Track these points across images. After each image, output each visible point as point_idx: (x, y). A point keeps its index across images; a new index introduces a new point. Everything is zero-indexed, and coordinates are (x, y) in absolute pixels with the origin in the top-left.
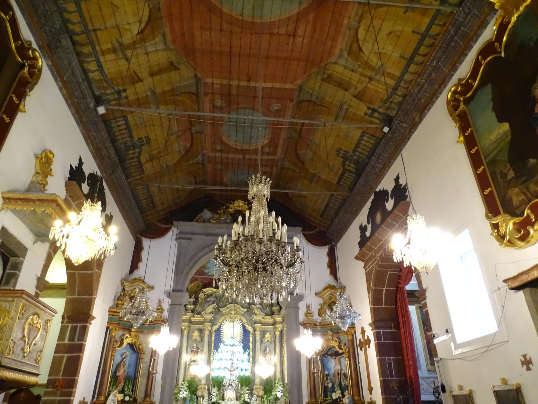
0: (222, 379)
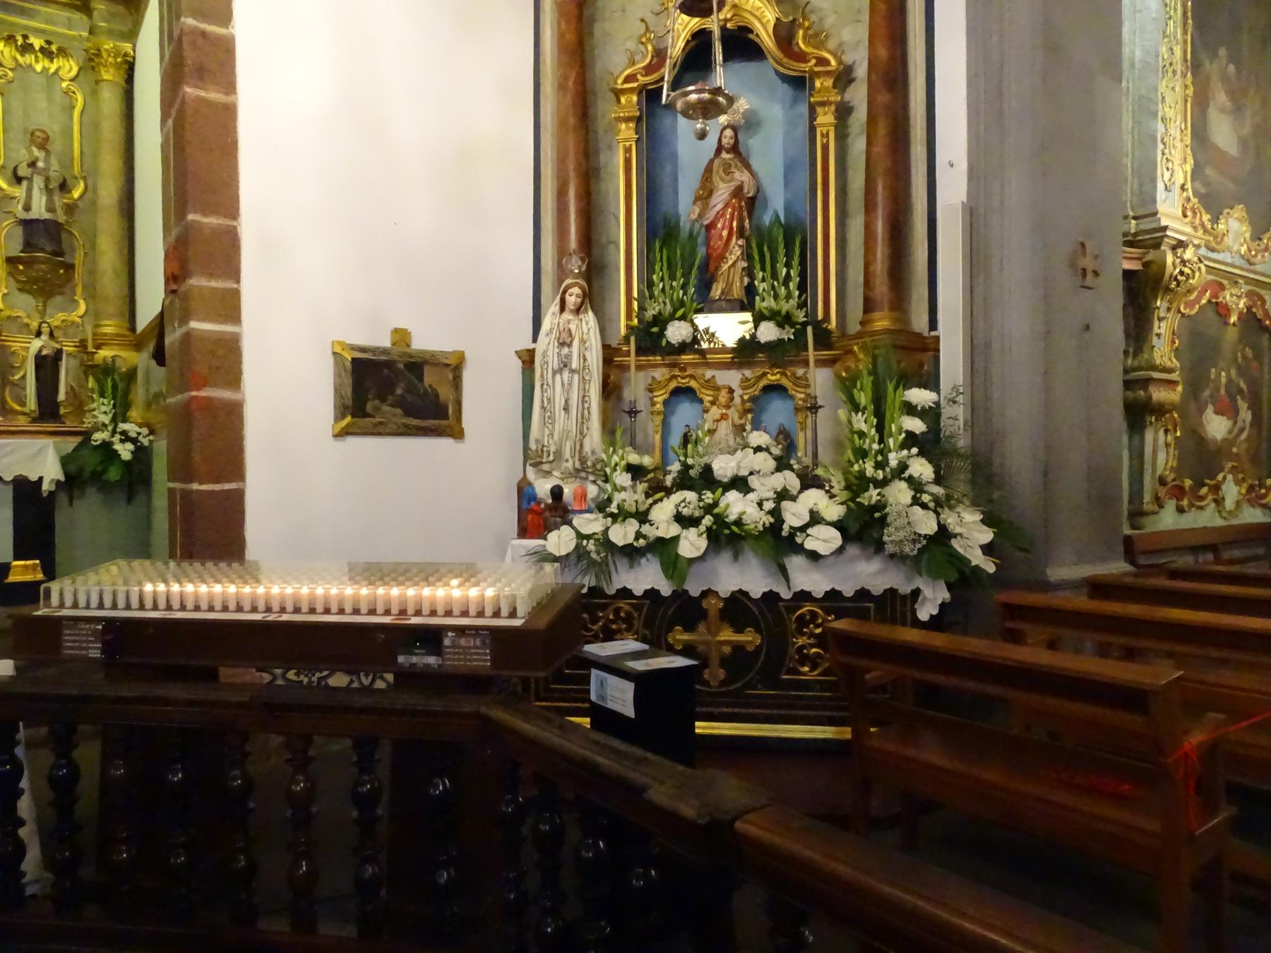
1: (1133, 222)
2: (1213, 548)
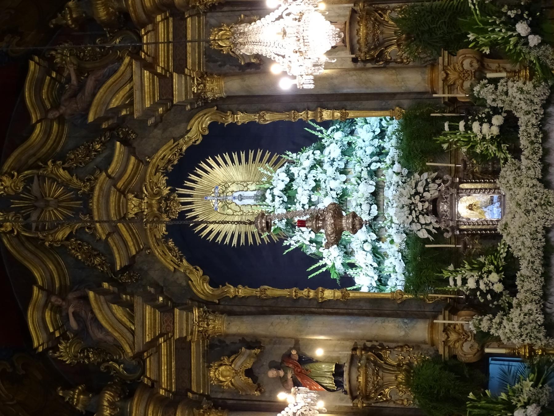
0: (412, 240)
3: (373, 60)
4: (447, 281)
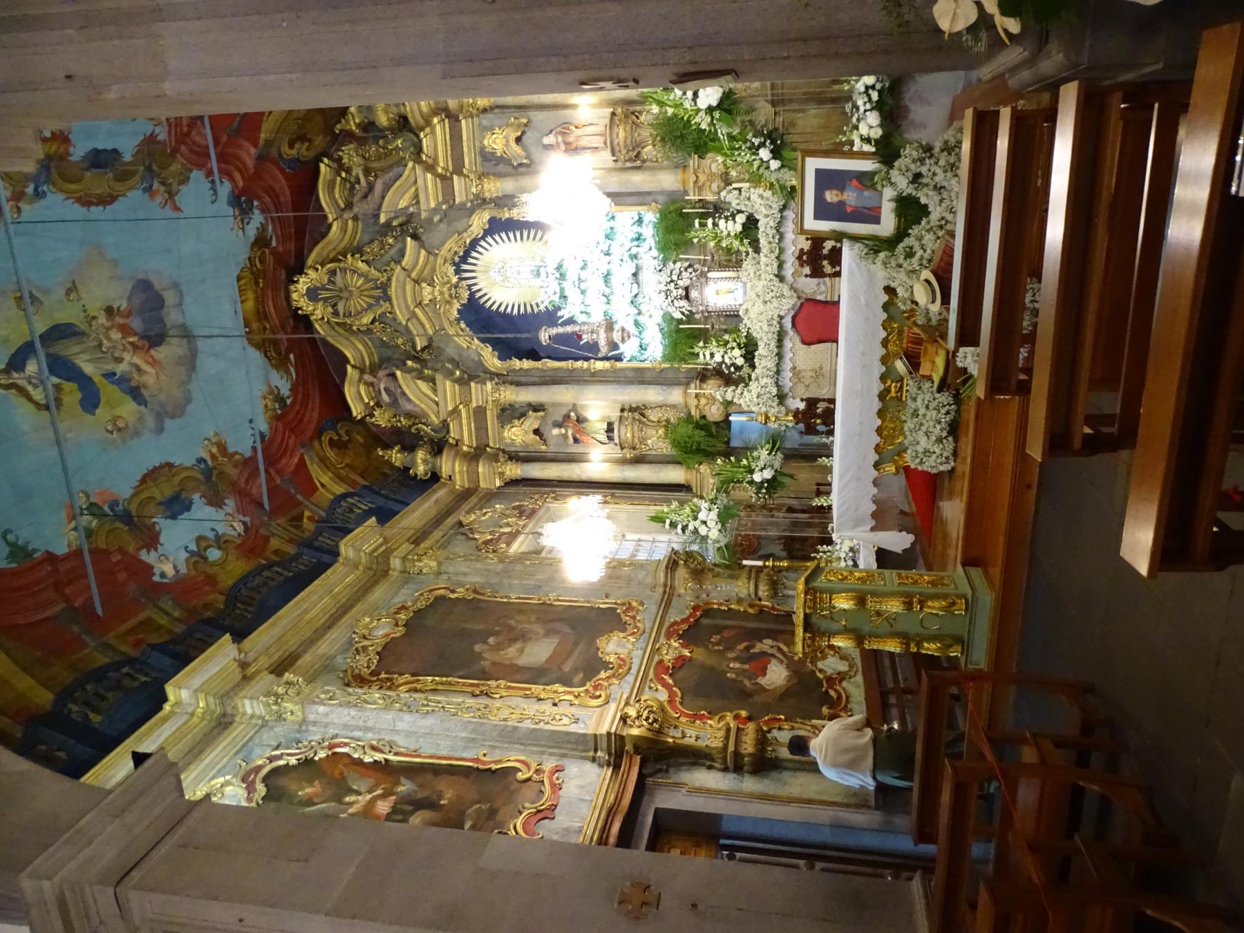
0: (668, 318)
1: (599, 753)
2: (884, 695)
3: (630, 160)
4: (698, 355)
